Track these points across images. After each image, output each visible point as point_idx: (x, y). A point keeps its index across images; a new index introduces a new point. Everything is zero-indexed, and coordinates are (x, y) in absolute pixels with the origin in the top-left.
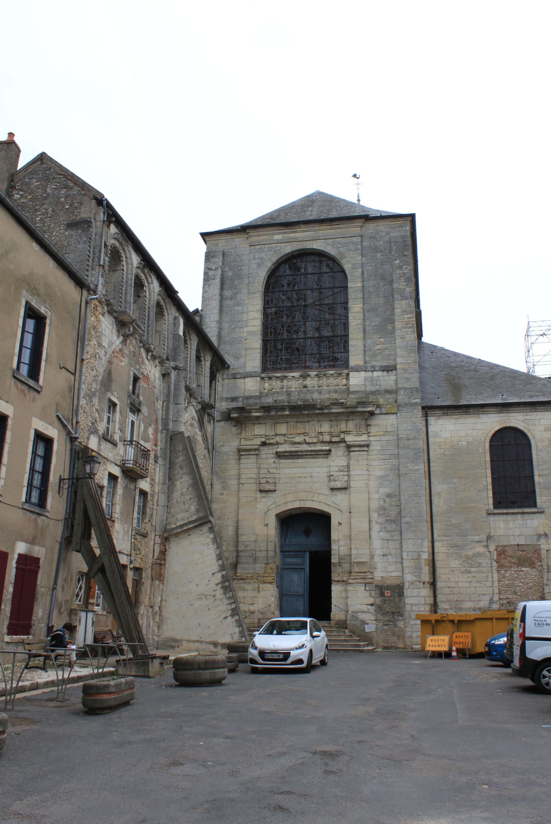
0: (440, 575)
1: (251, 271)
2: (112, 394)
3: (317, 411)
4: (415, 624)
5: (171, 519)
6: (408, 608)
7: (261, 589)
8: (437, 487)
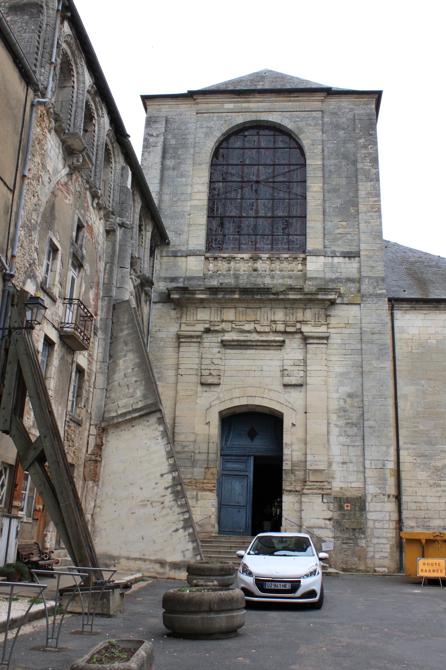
0: (405, 488)
1: (197, 140)
2: (55, 235)
3: (272, 297)
4: (378, 543)
5: (111, 406)
6: (370, 524)
7: (199, 497)
8: (402, 390)
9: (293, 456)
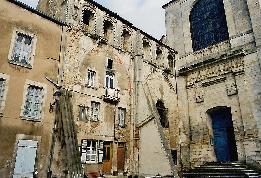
7: (203, 147)
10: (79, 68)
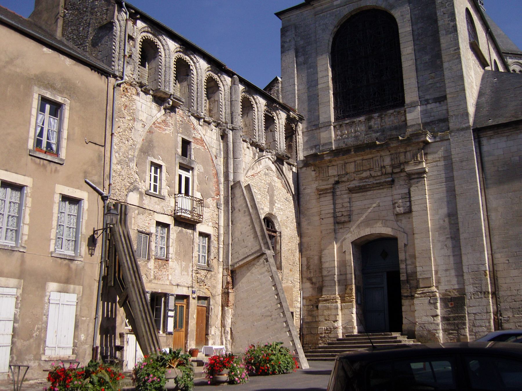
0: (501, 285)
1: (317, 36)
9: (408, 269)
10: (135, 159)
